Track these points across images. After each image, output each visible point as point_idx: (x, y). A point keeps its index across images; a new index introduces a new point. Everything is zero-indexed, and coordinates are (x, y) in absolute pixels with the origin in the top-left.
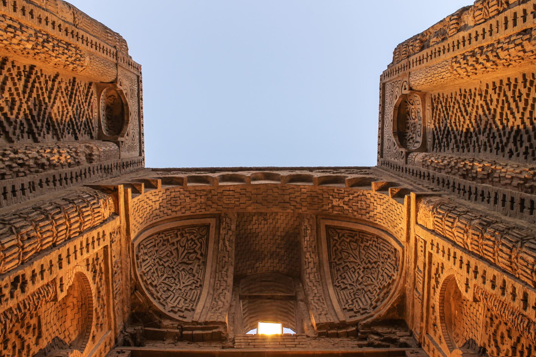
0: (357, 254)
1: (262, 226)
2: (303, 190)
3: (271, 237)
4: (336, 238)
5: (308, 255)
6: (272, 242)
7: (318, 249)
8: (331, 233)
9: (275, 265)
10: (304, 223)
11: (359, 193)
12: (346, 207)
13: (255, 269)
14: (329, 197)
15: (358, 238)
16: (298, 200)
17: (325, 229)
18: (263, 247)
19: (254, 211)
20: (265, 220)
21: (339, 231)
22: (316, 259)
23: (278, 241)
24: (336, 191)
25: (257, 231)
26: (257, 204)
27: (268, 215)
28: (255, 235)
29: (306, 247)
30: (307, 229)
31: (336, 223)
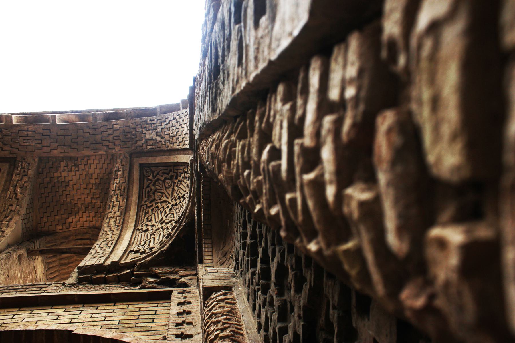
0: (170, 193)
1: (73, 173)
2: (115, 126)
3: (84, 186)
4: (150, 178)
5: (114, 199)
6: (87, 191)
7: (128, 192)
8: (145, 173)
9: (91, 220)
10: (117, 164)
11: (169, 119)
12: (159, 139)
13: (67, 225)
14: (142, 131)
15: (173, 174)
16: (111, 138)
17: (139, 169)
18: (76, 198)
19: (61, 155)
20: (76, 166)
21: (153, 169)
22: (123, 203)
23: (93, 191)
24: (149, 122)
25: (67, 179)
26: (65, 148)
27: (79, 160)
28: (64, 184)
29: (115, 190)
30: (119, 170)
31: (151, 160)
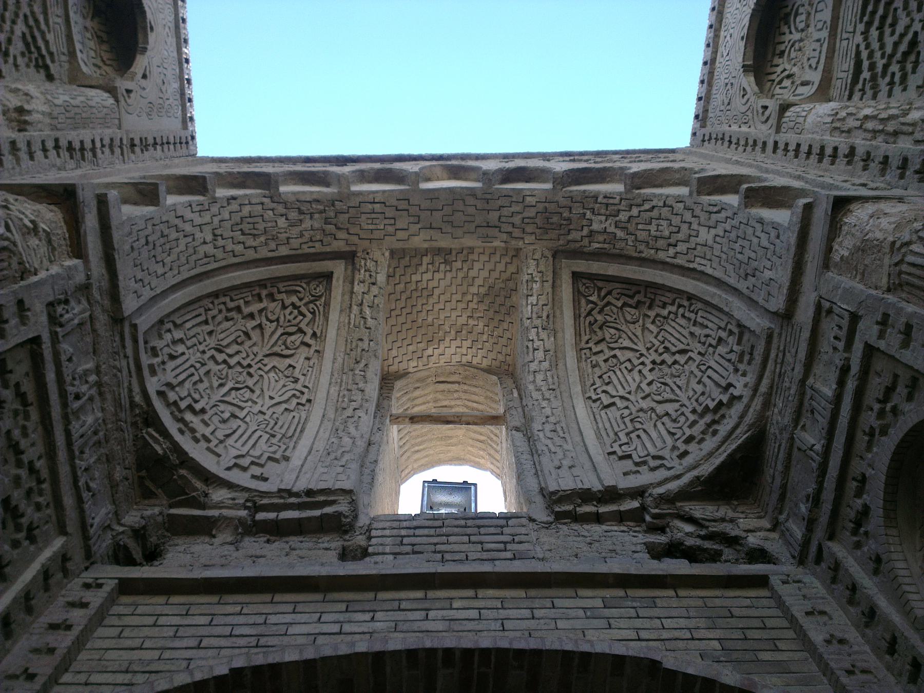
0: (639, 333)
1: (441, 275)
2: (528, 199)
4: (594, 298)
6: (461, 306)
8: (582, 289)
12: (620, 234)
14: (585, 214)
15: (644, 300)
16: (517, 220)
17: (570, 281)
18: (442, 317)
19: (426, 245)
20: (446, 262)
21: (600, 284)
26: (432, 231)
27: (454, 253)
28: (425, 293)
